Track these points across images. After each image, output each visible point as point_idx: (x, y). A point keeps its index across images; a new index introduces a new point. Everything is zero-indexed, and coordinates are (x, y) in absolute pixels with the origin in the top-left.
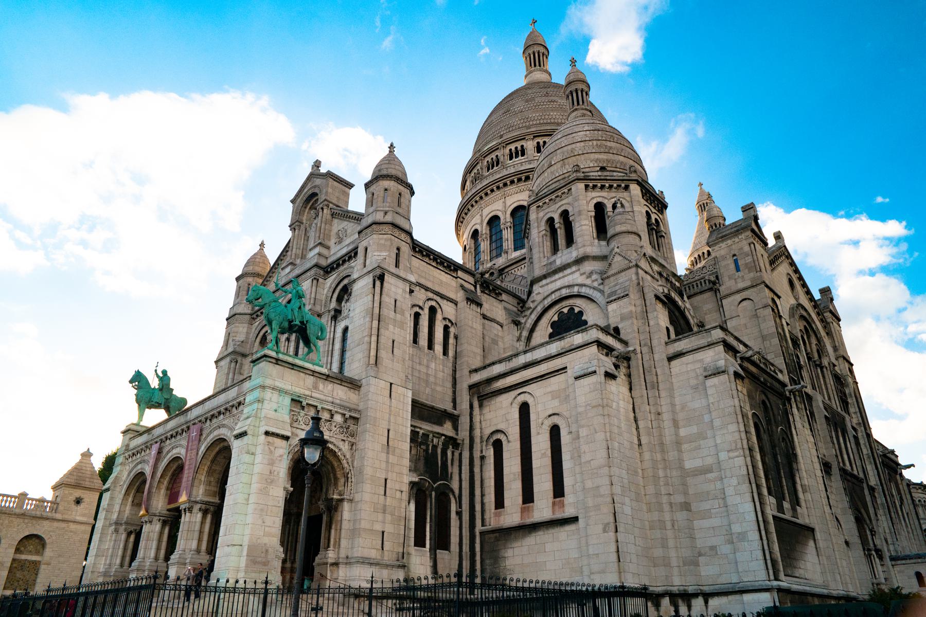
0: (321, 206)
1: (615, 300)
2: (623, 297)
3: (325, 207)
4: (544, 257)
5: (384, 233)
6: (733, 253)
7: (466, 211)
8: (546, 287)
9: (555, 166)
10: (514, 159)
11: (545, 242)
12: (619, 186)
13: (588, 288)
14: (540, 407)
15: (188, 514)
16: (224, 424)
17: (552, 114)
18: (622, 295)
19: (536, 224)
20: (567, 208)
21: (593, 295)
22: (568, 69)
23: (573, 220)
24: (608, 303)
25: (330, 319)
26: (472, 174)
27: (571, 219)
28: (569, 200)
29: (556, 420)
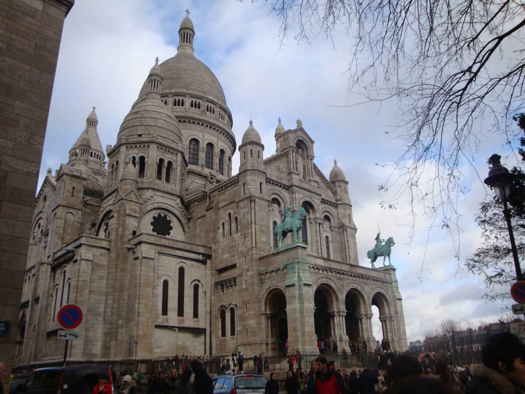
0: (312, 158)
7: (192, 122)
26: (194, 100)
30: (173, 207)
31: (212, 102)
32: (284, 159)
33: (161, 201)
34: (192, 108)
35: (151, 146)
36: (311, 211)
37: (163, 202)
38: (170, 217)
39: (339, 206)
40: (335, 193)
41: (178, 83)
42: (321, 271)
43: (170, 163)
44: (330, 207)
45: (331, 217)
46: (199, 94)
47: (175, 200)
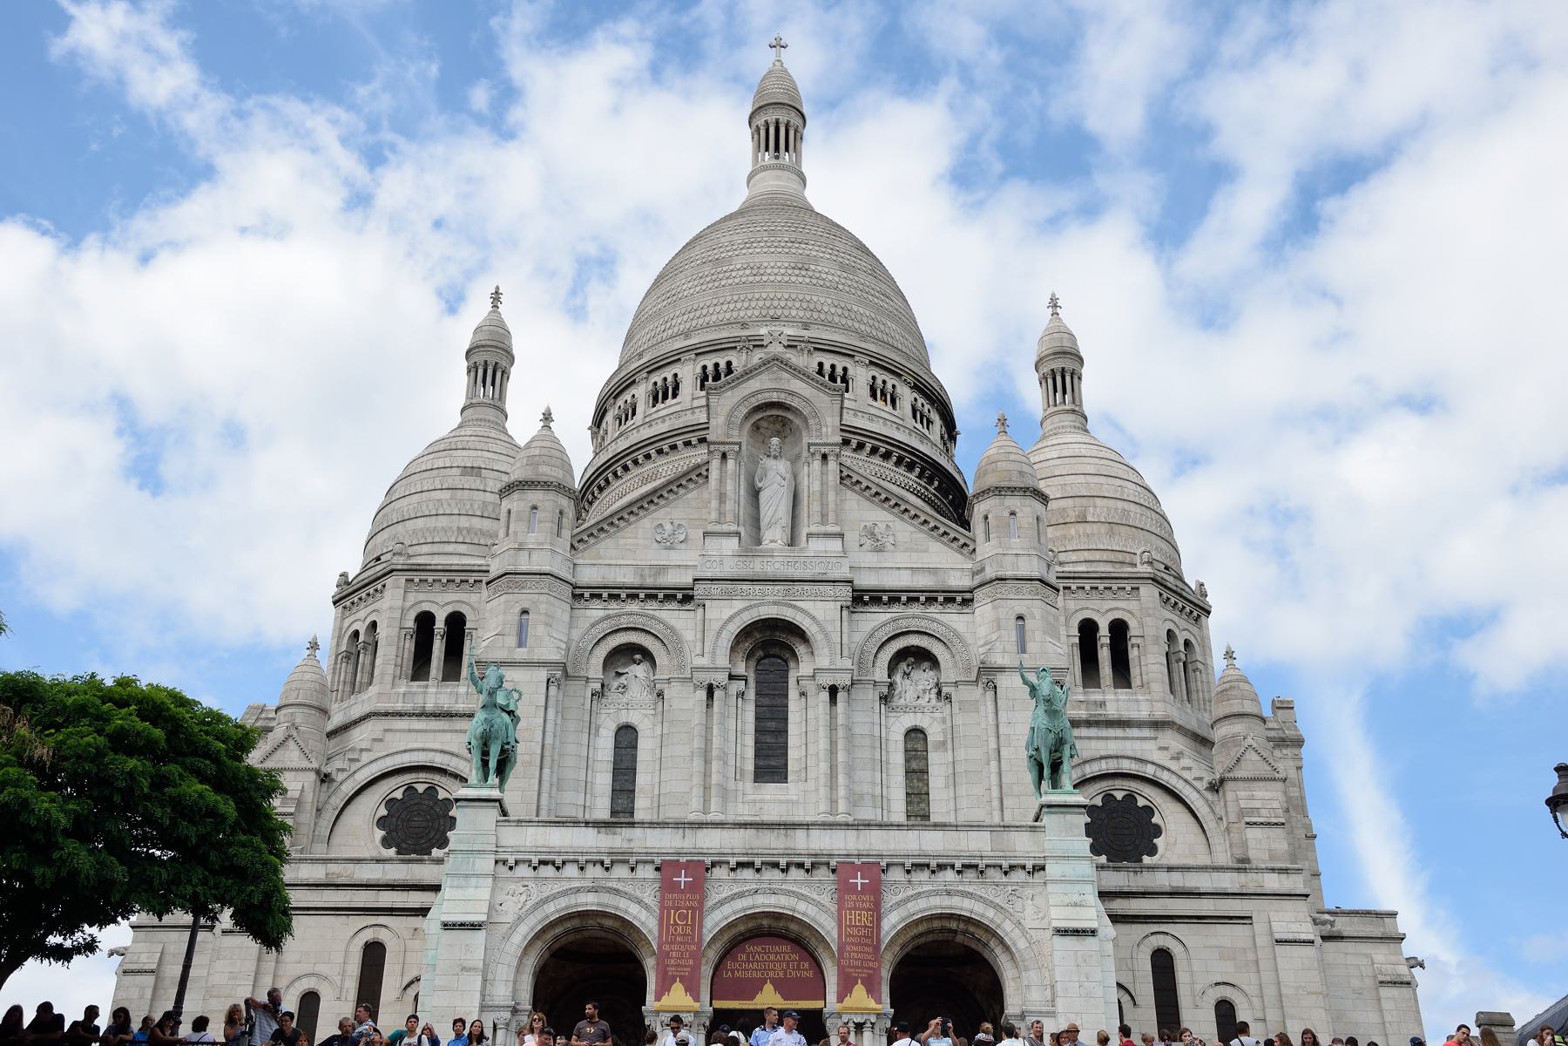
0: (824, 450)
1: (1262, 824)
2: (1276, 824)
5: (1051, 603)
8: (1086, 741)
9: (1095, 526)
11: (1076, 658)
12: (1191, 612)
13: (1174, 776)
14: (1196, 966)
15: (867, 1034)
16: (972, 894)
17: (889, 323)
20: (1126, 619)
21: (1184, 791)
24: (1247, 823)
26: (709, 362)
27: (1134, 641)
28: (1133, 605)
29: (1227, 993)
30: (452, 754)
32: (689, 496)
35: (389, 581)
36: (801, 650)
37: (420, 745)
39: (978, 594)
40: (967, 548)
41: (668, 325)
43: (456, 622)
46: (724, 334)
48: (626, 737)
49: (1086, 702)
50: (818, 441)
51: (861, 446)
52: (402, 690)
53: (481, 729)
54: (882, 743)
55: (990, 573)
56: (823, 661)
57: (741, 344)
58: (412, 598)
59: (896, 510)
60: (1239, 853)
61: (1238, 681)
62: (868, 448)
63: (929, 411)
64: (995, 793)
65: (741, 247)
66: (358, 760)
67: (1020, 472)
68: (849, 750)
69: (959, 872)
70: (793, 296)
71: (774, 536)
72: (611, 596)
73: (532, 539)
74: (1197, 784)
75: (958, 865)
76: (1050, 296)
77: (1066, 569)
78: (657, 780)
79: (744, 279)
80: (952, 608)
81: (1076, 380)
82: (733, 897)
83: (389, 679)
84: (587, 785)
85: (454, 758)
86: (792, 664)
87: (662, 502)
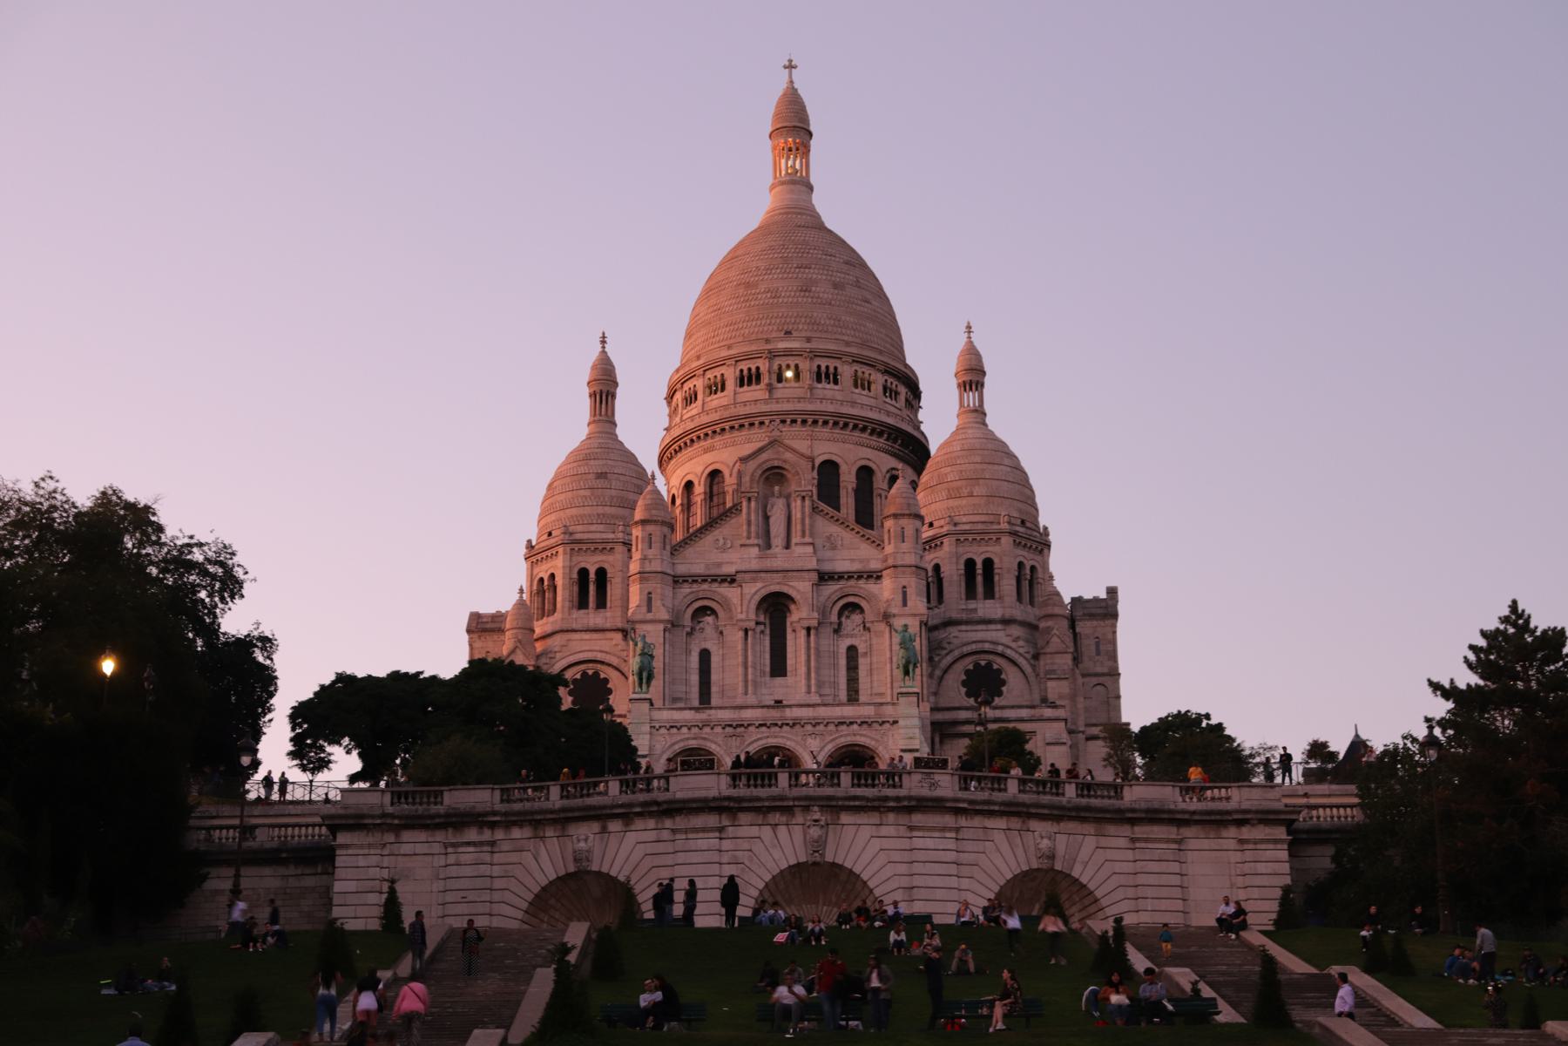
0: (804, 494)
3: (807, 498)
4: (961, 599)
6: (1096, 635)
7: (737, 426)
8: (964, 634)
10: (824, 385)
12: (1037, 548)
17: (868, 324)
18: (1063, 677)
19: (954, 560)
20: (992, 557)
22: (963, 339)
23: (999, 574)
25: (832, 630)
27: (996, 571)
28: (997, 549)
30: (606, 652)
31: (788, 353)
32: (733, 521)
33: (583, 649)
34: (742, 390)
36: (792, 607)
37: (587, 648)
38: (606, 673)
39: (884, 573)
42: (685, 730)
43: (601, 573)
44: (861, 582)
45: (863, 604)
46: (754, 348)
47: (612, 639)
48: (705, 656)
49: (967, 609)
50: (800, 489)
51: (846, 425)
52: (574, 616)
53: (638, 666)
54: (835, 655)
55: (890, 562)
56: (804, 615)
57: (764, 356)
58: (574, 559)
59: (842, 526)
60: (1043, 694)
61: (1054, 595)
62: (851, 426)
63: (896, 386)
64: (889, 680)
65: (764, 272)
66: (554, 658)
67: (909, 505)
68: (817, 661)
69: (860, 725)
70: (800, 314)
71: (778, 540)
72: (693, 581)
73: (651, 553)
74: (1026, 655)
75: (859, 721)
76: (966, 325)
77: (958, 528)
78: (721, 677)
79: (767, 301)
80: (872, 581)
81: (979, 386)
82: (755, 741)
83: (566, 610)
84: (687, 682)
85: (609, 656)
86: (788, 615)
87: (718, 525)
